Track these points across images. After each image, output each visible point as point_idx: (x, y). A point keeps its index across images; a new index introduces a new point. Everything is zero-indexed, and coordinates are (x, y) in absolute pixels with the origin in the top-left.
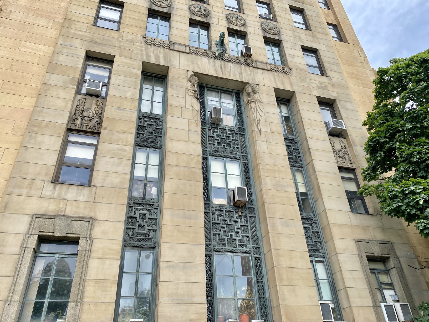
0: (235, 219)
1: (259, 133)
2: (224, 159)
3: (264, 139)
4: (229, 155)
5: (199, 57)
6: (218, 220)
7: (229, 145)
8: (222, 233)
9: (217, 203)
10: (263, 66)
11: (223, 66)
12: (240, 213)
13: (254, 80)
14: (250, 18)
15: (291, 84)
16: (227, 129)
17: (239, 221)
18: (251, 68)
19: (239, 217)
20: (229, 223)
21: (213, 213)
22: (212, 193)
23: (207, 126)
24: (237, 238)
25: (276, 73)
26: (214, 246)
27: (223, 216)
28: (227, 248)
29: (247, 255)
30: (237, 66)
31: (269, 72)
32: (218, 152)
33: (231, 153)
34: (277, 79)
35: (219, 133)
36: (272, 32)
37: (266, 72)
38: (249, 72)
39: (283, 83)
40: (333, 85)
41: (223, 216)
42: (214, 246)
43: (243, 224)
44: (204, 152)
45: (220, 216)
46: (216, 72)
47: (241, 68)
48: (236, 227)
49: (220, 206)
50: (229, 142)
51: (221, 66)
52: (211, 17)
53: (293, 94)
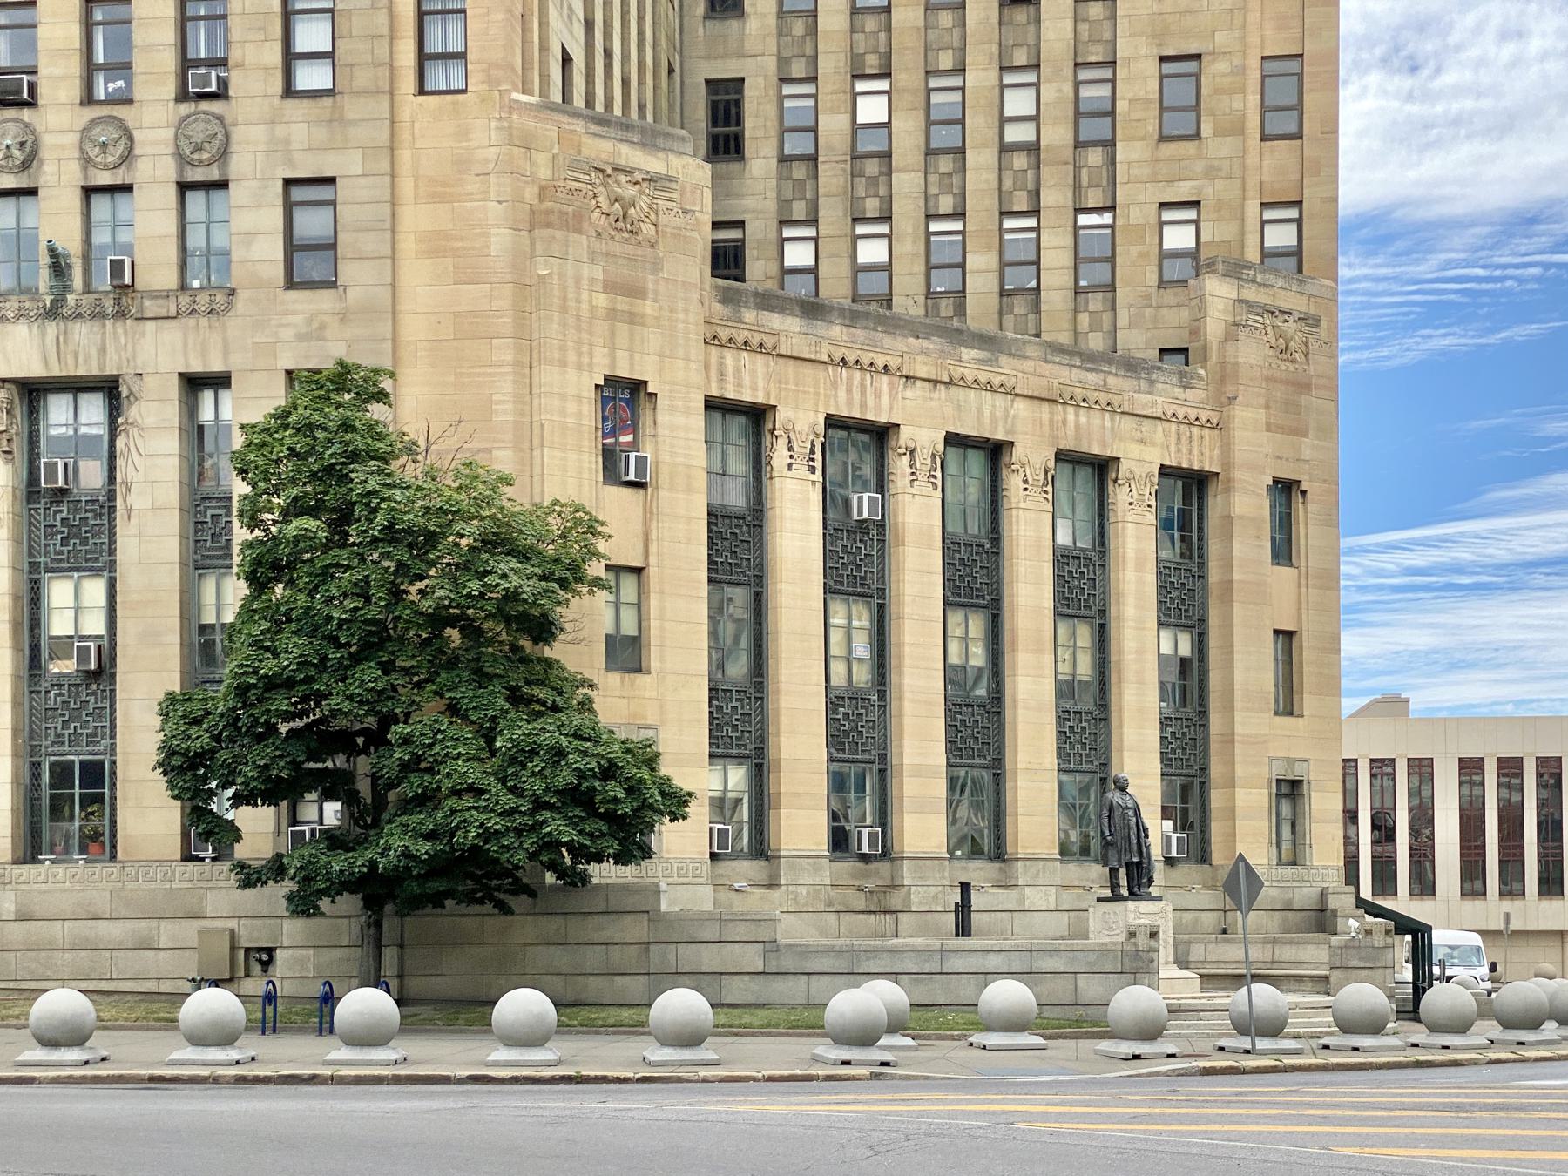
0: (84, 698)
1: (126, 517)
2: (76, 575)
3: (134, 531)
4: (84, 564)
5: (9, 327)
6: (56, 703)
7: (85, 541)
8: (59, 725)
9: (56, 670)
10: (159, 307)
11: (61, 339)
12: (94, 687)
13: (132, 363)
14: (147, 120)
15: (226, 352)
16: (83, 499)
17: (92, 700)
18: (128, 322)
19: (94, 693)
20: (72, 706)
21: (47, 692)
22: (45, 654)
23: (43, 501)
24: (85, 731)
25: (191, 321)
26: (47, 747)
27: (63, 695)
28: (67, 749)
29: (101, 757)
30: (96, 325)
31: (173, 323)
32: (61, 560)
33: (87, 560)
34: (190, 341)
35: (64, 515)
36: (201, 161)
37: (166, 323)
38: (122, 341)
39: (204, 353)
40: (344, 317)
41: (63, 695)
42: (47, 747)
43: (100, 705)
44: (34, 567)
45: (61, 694)
46: (46, 363)
47: (104, 333)
48: (84, 713)
49: (61, 675)
50: (86, 532)
51: (58, 338)
52: (41, 162)
53: (230, 372)
